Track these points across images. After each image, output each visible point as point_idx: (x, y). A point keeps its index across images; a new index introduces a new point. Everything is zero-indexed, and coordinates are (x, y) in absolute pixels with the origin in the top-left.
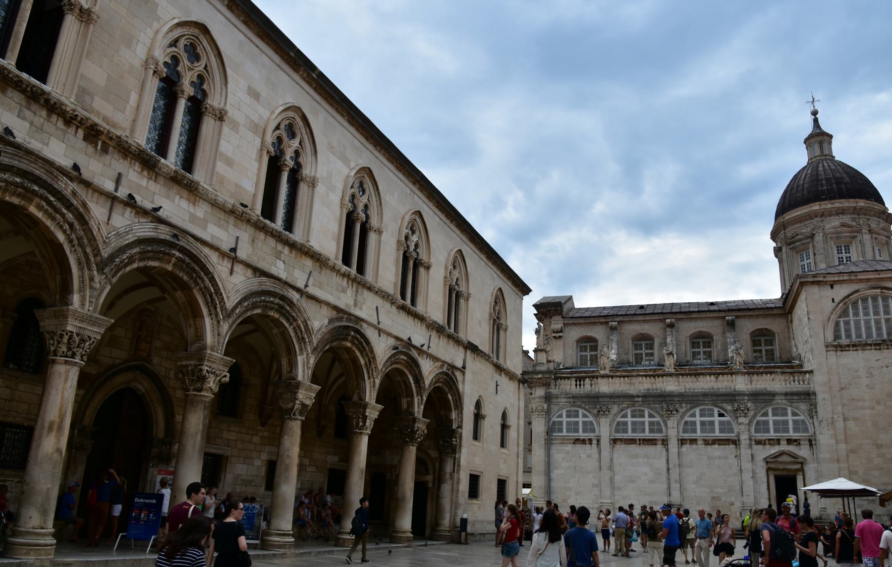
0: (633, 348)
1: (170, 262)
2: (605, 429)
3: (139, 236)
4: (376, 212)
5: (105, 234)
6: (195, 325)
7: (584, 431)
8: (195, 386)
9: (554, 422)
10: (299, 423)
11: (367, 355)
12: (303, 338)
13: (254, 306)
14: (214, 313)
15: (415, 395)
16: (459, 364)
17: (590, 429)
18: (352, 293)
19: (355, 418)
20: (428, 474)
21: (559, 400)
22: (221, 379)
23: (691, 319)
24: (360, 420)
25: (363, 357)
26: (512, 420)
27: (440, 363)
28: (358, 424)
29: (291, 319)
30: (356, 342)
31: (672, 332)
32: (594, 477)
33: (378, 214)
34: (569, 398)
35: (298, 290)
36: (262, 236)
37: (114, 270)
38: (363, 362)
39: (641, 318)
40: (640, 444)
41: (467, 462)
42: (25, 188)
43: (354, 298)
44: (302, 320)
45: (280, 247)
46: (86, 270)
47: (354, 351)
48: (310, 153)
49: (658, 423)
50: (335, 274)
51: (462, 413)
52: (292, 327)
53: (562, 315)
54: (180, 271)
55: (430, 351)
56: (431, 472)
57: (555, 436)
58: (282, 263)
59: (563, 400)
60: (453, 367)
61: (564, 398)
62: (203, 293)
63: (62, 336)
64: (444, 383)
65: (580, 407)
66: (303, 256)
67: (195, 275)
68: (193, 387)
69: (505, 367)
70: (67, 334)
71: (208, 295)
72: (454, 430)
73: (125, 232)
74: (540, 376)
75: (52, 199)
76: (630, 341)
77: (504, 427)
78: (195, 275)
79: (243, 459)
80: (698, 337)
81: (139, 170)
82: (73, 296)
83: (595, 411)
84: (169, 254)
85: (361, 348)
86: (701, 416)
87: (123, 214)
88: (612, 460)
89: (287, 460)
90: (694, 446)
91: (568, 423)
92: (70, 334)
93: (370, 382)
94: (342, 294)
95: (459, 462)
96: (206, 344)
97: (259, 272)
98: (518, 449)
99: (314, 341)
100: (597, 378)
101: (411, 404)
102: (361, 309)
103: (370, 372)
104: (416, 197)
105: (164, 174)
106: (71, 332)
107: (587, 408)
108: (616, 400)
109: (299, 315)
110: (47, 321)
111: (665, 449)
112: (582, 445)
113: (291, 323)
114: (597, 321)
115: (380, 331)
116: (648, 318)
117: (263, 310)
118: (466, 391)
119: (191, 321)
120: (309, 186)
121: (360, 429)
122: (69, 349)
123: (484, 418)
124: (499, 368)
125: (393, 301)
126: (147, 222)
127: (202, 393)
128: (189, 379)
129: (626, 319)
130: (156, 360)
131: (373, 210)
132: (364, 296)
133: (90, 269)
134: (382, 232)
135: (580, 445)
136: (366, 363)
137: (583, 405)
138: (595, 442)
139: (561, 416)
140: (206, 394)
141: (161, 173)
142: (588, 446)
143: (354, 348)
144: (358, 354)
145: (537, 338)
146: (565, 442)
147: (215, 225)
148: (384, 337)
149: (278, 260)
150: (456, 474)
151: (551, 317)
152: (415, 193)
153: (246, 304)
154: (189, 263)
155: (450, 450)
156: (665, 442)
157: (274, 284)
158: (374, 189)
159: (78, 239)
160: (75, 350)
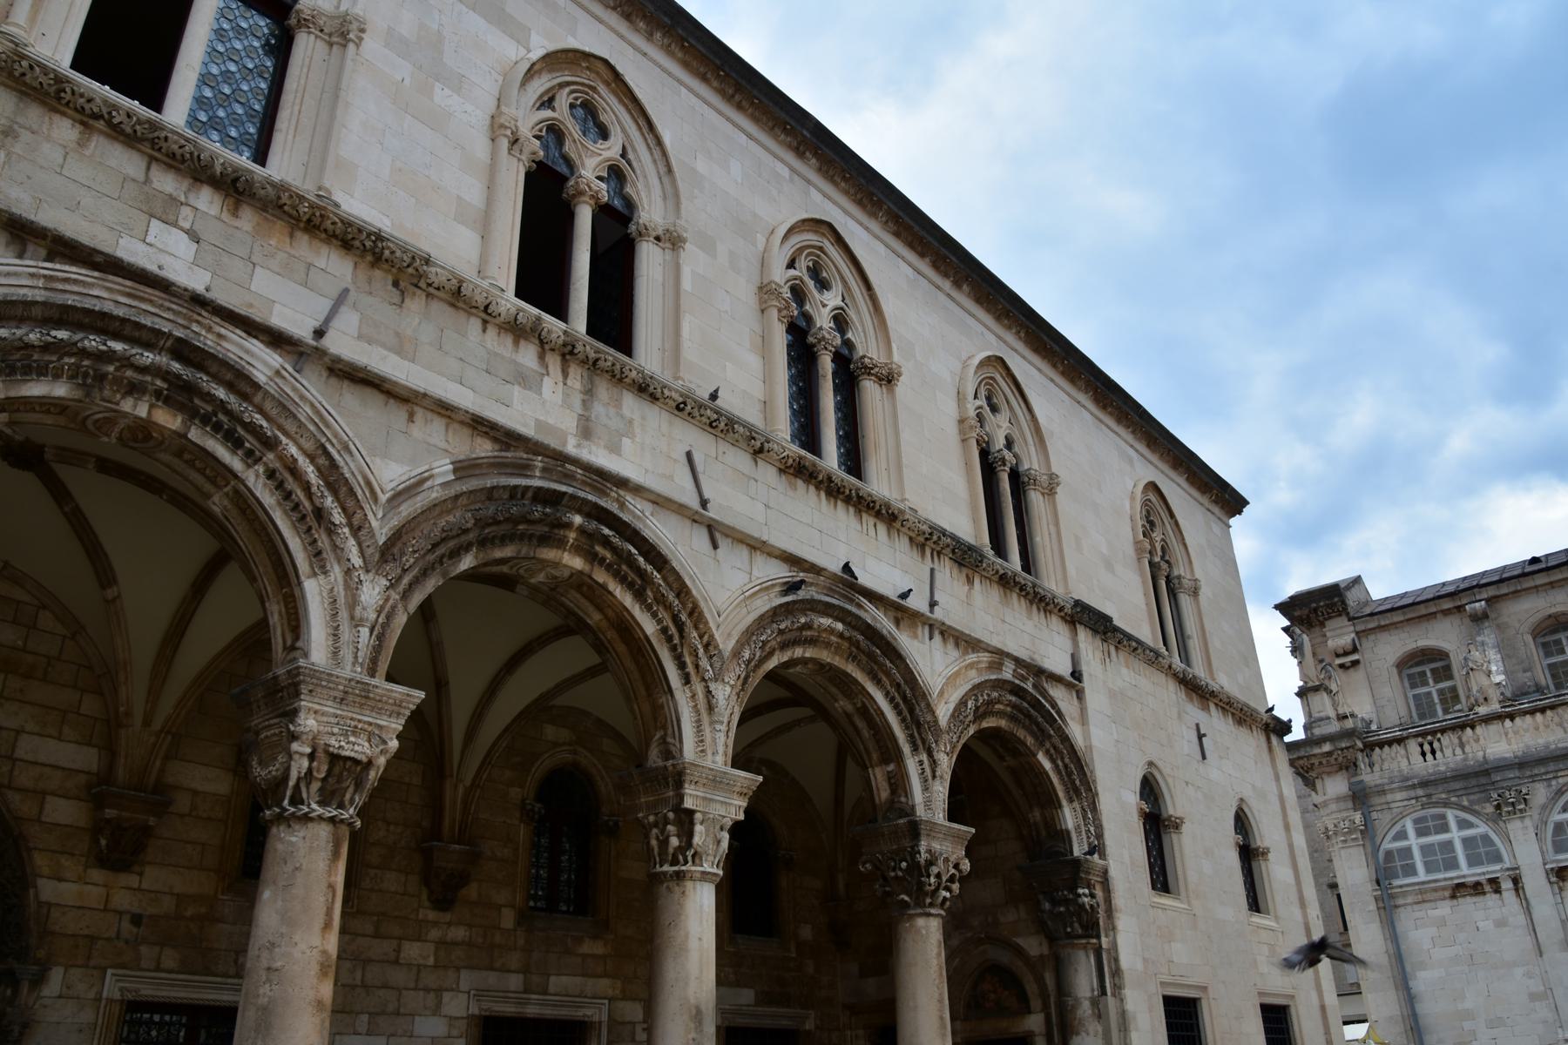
0: (1541, 654)
7: (1473, 861)
9: (1389, 854)
11: (661, 600)
12: (320, 513)
15: (906, 749)
16: (1059, 664)
17: (1487, 853)
18: (566, 395)
19: (656, 825)
20: (1028, 1011)
21: (1389, 797)
24: (670, 828)
26: (1268, 833)
27: (985, 657)
28: (664, 843)
29: (257, 444)
32: (1529, 975)
33: (665, 198)
34: (1413, 787)
35: (277, 339)
36: (65, 130)
38: (649, 627)
41: (1145, 960)
43: (578, 408)
44: (309, 446)
45: (166, 183)
47: (604, 587)
51: (1094, 808)
53: (1348, 614)
55: (938, 614)
56: (1036, 1003)
57: (1401, 887)
59: (1399, 796)
60: (1039, 672)
61: (1401, 789)
64: (1012, 718)
65: (1446, 804)
66: (303, 239)
69: (1216, 688)
72: (1077, 863)
74: (1327, 747)
76: (1529, 638)
77: (1249, 854)
79: (365, 1018)
83: (1489, 809)
85: (632, 576)
89: (265, 990)
91: (1426, 850)
93: (693, 696)
94: (517, 391)
95: (1116, 960)
98: (1305, 915)
99: (375, 524)
100: (1473, 728)
101: (899, 783)
102: (615, 449)
103: (688, 659)
104: (814, 193)
107: (1465, 803)
108: (1536, 771)
109: (291, 427)
112: (1475, 899)
113: (249, 453)
114: (1433, 609)
115: (715, 531)
118: (1095, 742)
120: (331, 45)
121: (675, 862)
123: (1177, 827)
129: (1504, 589)
131: (647, 186)
132: (626, 411)
134: (684, 241)
136: (664, 630)
137: (1453, 799)
138: (1507, 885)
142: (1491, 899)
143: (601, 576)
144: (627, 600)
145: (1300, 663)
146: (1428, 896)
148: (733, 560)
149: (155, 223)
150: (1111, 1000)
151: (1322, 625)
152: (809, 182)
155: (1076, 925)
157: (129, 295)
158: (640, 128)
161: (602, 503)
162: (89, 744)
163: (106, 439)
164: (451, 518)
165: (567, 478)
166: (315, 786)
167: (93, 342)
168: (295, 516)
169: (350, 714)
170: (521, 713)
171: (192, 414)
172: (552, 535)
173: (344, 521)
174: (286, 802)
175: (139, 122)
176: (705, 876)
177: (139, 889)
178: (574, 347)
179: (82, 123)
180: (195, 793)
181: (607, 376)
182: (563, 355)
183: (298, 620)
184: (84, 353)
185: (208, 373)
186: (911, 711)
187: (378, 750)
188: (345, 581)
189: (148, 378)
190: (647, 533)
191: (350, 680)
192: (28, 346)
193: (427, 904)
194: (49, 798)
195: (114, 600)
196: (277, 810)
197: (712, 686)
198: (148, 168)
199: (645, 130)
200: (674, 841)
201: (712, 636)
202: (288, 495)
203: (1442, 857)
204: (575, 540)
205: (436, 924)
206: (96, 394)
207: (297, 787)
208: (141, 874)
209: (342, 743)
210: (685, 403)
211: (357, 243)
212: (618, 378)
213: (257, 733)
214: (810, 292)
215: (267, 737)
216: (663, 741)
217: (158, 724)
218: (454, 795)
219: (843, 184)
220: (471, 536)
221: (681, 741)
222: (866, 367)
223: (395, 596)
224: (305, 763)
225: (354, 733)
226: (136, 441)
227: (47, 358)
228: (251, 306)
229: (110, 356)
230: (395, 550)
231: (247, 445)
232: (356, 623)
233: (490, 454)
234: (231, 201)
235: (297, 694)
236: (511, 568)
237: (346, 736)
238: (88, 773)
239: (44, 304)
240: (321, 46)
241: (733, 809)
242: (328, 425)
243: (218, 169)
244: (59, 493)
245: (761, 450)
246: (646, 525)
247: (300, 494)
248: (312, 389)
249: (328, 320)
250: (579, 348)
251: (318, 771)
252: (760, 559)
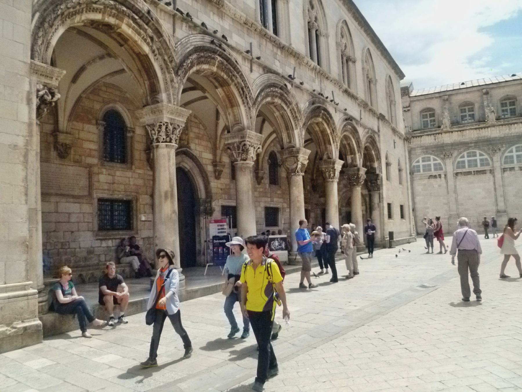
1: (215, 64)
2: (449, 167)
3: (195, 45)
4: (322, 22)
5: (174, 45)
6: (233, 112)
8: (241, 157)
9: (414, 166)
10: (301, 177)
11: (331, 127)
12: (296, 117)
16: (376, 129)
22: (257, 150)
23: (500, 87)
25: (329, 128)
28: (330, 175)
29: (288, 103)
30: (325, 117)
31: (487, 98)
37: (184, 72)
38: (329, 132)
39: (464, 91)
40: (474, 174)
42: (117, 9)
45: (275, 50)
46: (167, 73)
49: (486, 159)
51: (381, 162)
52: (289, 109)
54: (222, 71)
58: (278, 62)
60: (374, 132)
62: (237, 87)
63: (160, 126)
64: (370, 143)
65: (431, 154)
67: (230, 74)
68: (240, 158)
70: (164, 124)
73: (186, 42)
75: (137, 17)
78: (230, 74)
80: (505, 100)
82: (162, 95)
84: (214, 58)
86: (517, 151)
87: (182, 28)
88: (455, 186)
90: (513, 172)
91: (424, 166)
92: (166, 124)
95: (383, 195)
96: (244, 126)
100: (441, 134)
103: (334, 138)
106: (166, 123)
110: (146, 117)
111: (492, 176)
116: (469, 90)
117: (272, 99)
119: (230, 110)
121: (332, 179)
122: (167, 136)
123: (390, 165)
124: (394, 131)
125: (340, 87)
126: (197, 34)
128: (235, 153)
130: (192, 146)
133: (169, 73)
135: (433, 179)
136: (331, 132)
138: (443, 176)
139: (418, 162)
142: (438, 179)
144: (326, 125)
147: (237, 34)
153: (263, 94)
156: (492, 172)
159: (158, 49)
160: (171, 136)
186: (359, 144)
200: (332, 175)
203: (427, 168)
216: (328, 154)
221: (332, 155)
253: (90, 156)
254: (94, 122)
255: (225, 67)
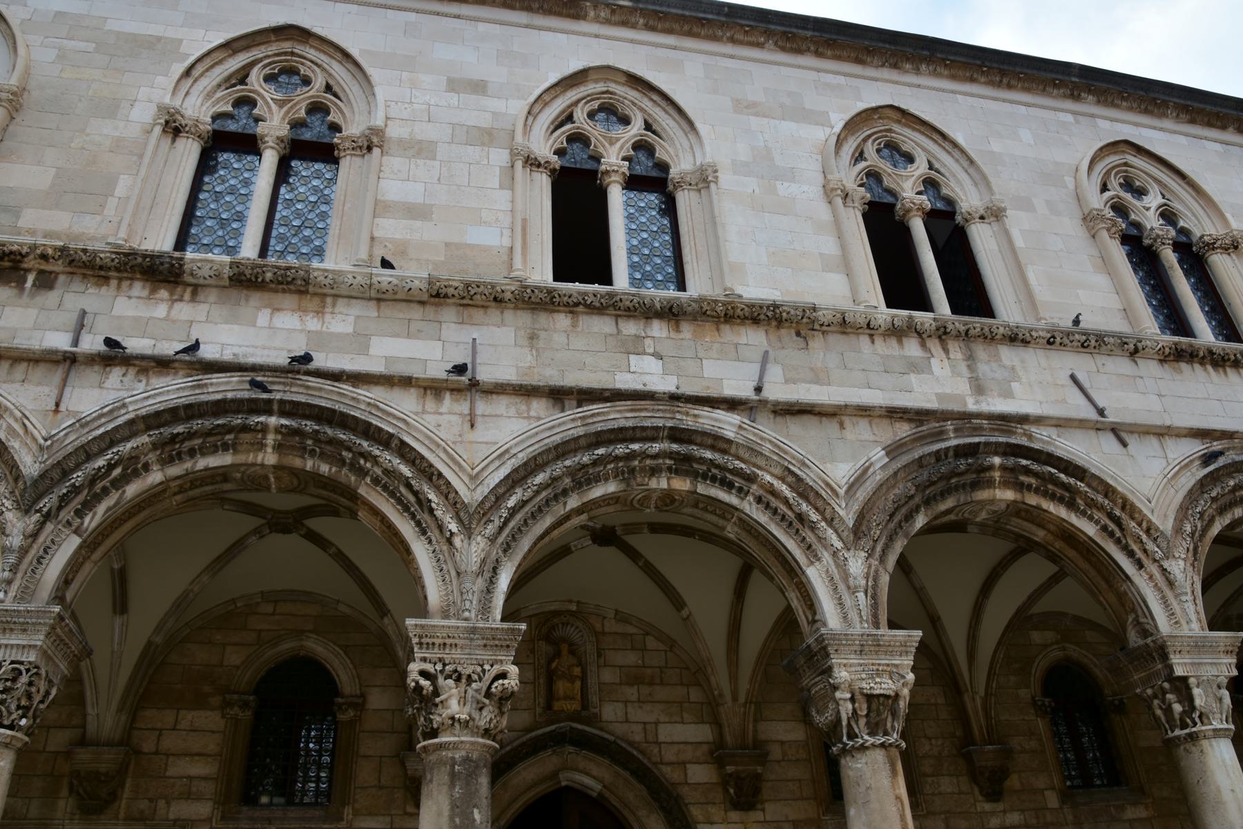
11: (1092, 504)
12: (801, 517)
13: (583, 478)
14: (433, 526)
18: (953, 367)
19: (1155, 696)
22: (489, 687)
24: (1169, 696)
28: (1168, 710)
33: (976, 184)
35: (732, 404)
36: (563, 320)
38: (1090, 529)
45: (631, 328)
47: (1038, 508)
48: (680, 133)
50: (865, 340)
52: (751, 498)
54: (302, 457)
62: (385, 488)
66: (726, 328)
67: (347, 455)
71: (402, 489)
78: (347, 455)
81: (145, 293)
84: (245, 428)
85: (1059, 492)
93: (1151, 577)
94: (913, 378)
97: (558, 395)
99: (842, 513)
102: (1008, 394)
103: (1135, 547)
104: (1100, 122)
105: (209, 281)
113: (740, 490)
115: (1117, 431)
120: (699, 191)
121: (1184, 726)
127: (444, 739)
130: (610, 712)
131: (958, 182)
134: (1004, 210)
136: (1104, 528)
140: (452, 739)
141: (201, 281)
143: (1032, 500)
144: (1062, 512)
147: (397, 335)
149: (632, 357)
152: (1092, 116)
154: (317, 432)
157: (632, 410)
161: (1013, 440)
162: (703, 722)
163: (648, 510)
164: (897, 491)
165: (977, 430)
166: (862, 722)
167: (620, 450)
168: (785, 524)
169: (871, 661)
170: (1007, 627)
171: (695, 475)
172: (980, 478)
173: (819, 518)
174: (845, 739)
175: (602, 297)
176: (1217, 733)
177: (765, 821)
178: (945, 327)
179: (571, 312)
180: (782, 743)
181: (981, 340)
182: (940, 337)
183: (811, 599)
184: (617, 458)
185: (696, 444)
187: (900, 684)
188: (835, 562)
189: (661, 461)
190: (1059, 453)
191: (862, 635)
192: (584, 466)
193: (980, 798)
194: (688, 766)
195: (688, 617)
196: (841, 746)
197: (1166, 564)
198: (617, 324)
199: (940, 140)
200: (1177, 708)
201: (1149, 521)
202: (775, 511)
204: (1001, 477)
205: (993, 813)
206: (633, 483)
207: (849, 725)
208: (763, 810)
209: (872, 685)
210: (1053, 337)
211: (762, 317)
212: (989, 338)
213: (809, 690)
214: (1130, 203)
215: (816, 692)
216: (1137, 623)
217: (742, 700)
218: (974, 705)
219: (1124, 104)
220: (917, 500)
221: (1153, 618)
222: (1208, 244)
223: (875, 563)
224: (850, 706)
225: (878, 675)
226: (666, 505)
227: (597, 469)
228: (708, 388)
229: (631, 456)
230: (864, 528)
231: (737, 484)
232: (853, 591)
233: (909, 433)
234: (673, 323)
235: (827, 655)
236: (957, 515)
237: (873, 678)
238: (708, 743)
239: (585, 435)
240: (693, 195)
241: (1226, 667)
242: (786, 453)
243: (658, 306)
244: (632, 554)
245: (1136, 351)
246: (1057, 447)
247: (783, 508)
248: (767, 431)
249: (761, 378)
250: (950, 327)
251: (861, 710)
252: (1170, 443)
253: (188, 796)
254: (216, 700)
255: (317, 441)
